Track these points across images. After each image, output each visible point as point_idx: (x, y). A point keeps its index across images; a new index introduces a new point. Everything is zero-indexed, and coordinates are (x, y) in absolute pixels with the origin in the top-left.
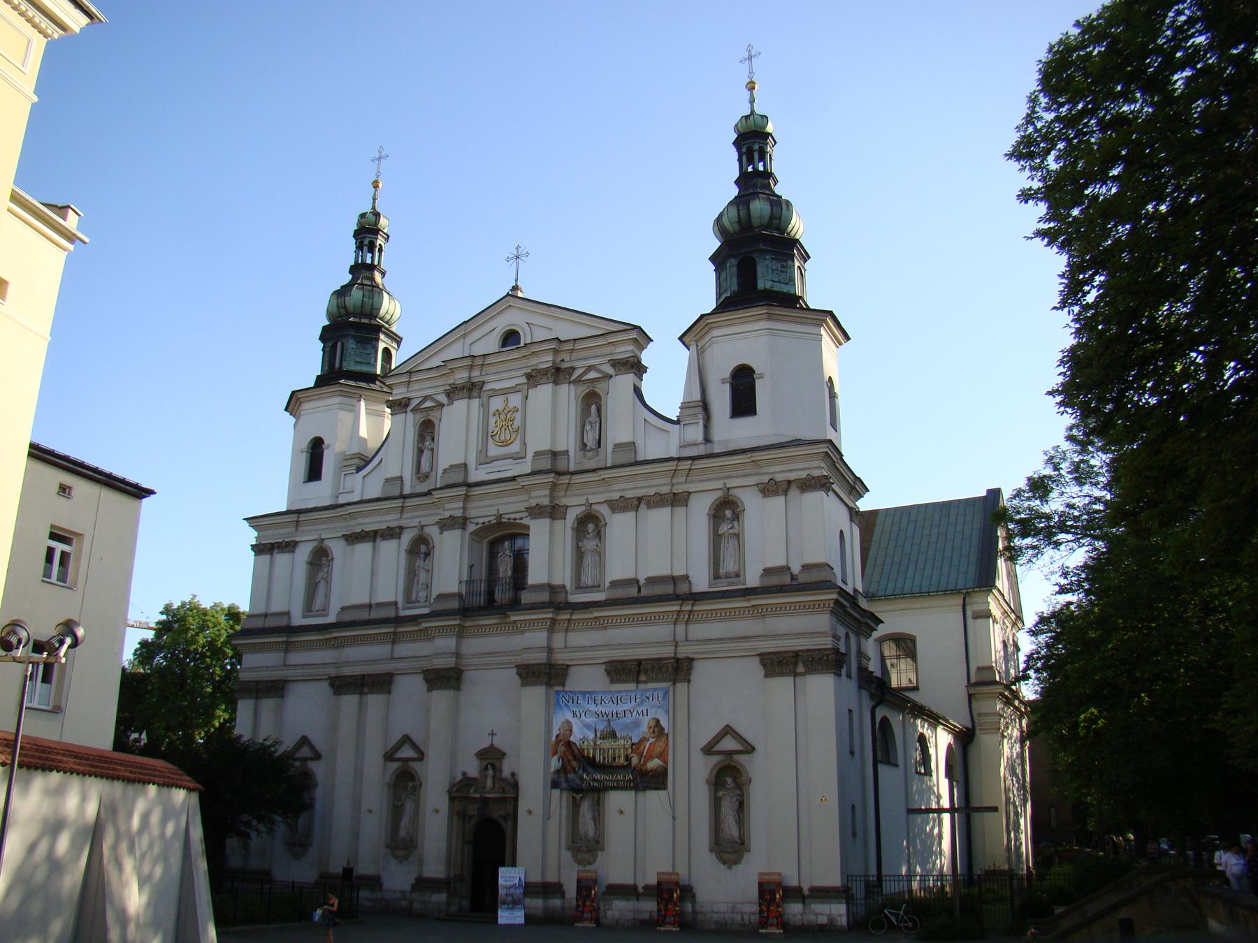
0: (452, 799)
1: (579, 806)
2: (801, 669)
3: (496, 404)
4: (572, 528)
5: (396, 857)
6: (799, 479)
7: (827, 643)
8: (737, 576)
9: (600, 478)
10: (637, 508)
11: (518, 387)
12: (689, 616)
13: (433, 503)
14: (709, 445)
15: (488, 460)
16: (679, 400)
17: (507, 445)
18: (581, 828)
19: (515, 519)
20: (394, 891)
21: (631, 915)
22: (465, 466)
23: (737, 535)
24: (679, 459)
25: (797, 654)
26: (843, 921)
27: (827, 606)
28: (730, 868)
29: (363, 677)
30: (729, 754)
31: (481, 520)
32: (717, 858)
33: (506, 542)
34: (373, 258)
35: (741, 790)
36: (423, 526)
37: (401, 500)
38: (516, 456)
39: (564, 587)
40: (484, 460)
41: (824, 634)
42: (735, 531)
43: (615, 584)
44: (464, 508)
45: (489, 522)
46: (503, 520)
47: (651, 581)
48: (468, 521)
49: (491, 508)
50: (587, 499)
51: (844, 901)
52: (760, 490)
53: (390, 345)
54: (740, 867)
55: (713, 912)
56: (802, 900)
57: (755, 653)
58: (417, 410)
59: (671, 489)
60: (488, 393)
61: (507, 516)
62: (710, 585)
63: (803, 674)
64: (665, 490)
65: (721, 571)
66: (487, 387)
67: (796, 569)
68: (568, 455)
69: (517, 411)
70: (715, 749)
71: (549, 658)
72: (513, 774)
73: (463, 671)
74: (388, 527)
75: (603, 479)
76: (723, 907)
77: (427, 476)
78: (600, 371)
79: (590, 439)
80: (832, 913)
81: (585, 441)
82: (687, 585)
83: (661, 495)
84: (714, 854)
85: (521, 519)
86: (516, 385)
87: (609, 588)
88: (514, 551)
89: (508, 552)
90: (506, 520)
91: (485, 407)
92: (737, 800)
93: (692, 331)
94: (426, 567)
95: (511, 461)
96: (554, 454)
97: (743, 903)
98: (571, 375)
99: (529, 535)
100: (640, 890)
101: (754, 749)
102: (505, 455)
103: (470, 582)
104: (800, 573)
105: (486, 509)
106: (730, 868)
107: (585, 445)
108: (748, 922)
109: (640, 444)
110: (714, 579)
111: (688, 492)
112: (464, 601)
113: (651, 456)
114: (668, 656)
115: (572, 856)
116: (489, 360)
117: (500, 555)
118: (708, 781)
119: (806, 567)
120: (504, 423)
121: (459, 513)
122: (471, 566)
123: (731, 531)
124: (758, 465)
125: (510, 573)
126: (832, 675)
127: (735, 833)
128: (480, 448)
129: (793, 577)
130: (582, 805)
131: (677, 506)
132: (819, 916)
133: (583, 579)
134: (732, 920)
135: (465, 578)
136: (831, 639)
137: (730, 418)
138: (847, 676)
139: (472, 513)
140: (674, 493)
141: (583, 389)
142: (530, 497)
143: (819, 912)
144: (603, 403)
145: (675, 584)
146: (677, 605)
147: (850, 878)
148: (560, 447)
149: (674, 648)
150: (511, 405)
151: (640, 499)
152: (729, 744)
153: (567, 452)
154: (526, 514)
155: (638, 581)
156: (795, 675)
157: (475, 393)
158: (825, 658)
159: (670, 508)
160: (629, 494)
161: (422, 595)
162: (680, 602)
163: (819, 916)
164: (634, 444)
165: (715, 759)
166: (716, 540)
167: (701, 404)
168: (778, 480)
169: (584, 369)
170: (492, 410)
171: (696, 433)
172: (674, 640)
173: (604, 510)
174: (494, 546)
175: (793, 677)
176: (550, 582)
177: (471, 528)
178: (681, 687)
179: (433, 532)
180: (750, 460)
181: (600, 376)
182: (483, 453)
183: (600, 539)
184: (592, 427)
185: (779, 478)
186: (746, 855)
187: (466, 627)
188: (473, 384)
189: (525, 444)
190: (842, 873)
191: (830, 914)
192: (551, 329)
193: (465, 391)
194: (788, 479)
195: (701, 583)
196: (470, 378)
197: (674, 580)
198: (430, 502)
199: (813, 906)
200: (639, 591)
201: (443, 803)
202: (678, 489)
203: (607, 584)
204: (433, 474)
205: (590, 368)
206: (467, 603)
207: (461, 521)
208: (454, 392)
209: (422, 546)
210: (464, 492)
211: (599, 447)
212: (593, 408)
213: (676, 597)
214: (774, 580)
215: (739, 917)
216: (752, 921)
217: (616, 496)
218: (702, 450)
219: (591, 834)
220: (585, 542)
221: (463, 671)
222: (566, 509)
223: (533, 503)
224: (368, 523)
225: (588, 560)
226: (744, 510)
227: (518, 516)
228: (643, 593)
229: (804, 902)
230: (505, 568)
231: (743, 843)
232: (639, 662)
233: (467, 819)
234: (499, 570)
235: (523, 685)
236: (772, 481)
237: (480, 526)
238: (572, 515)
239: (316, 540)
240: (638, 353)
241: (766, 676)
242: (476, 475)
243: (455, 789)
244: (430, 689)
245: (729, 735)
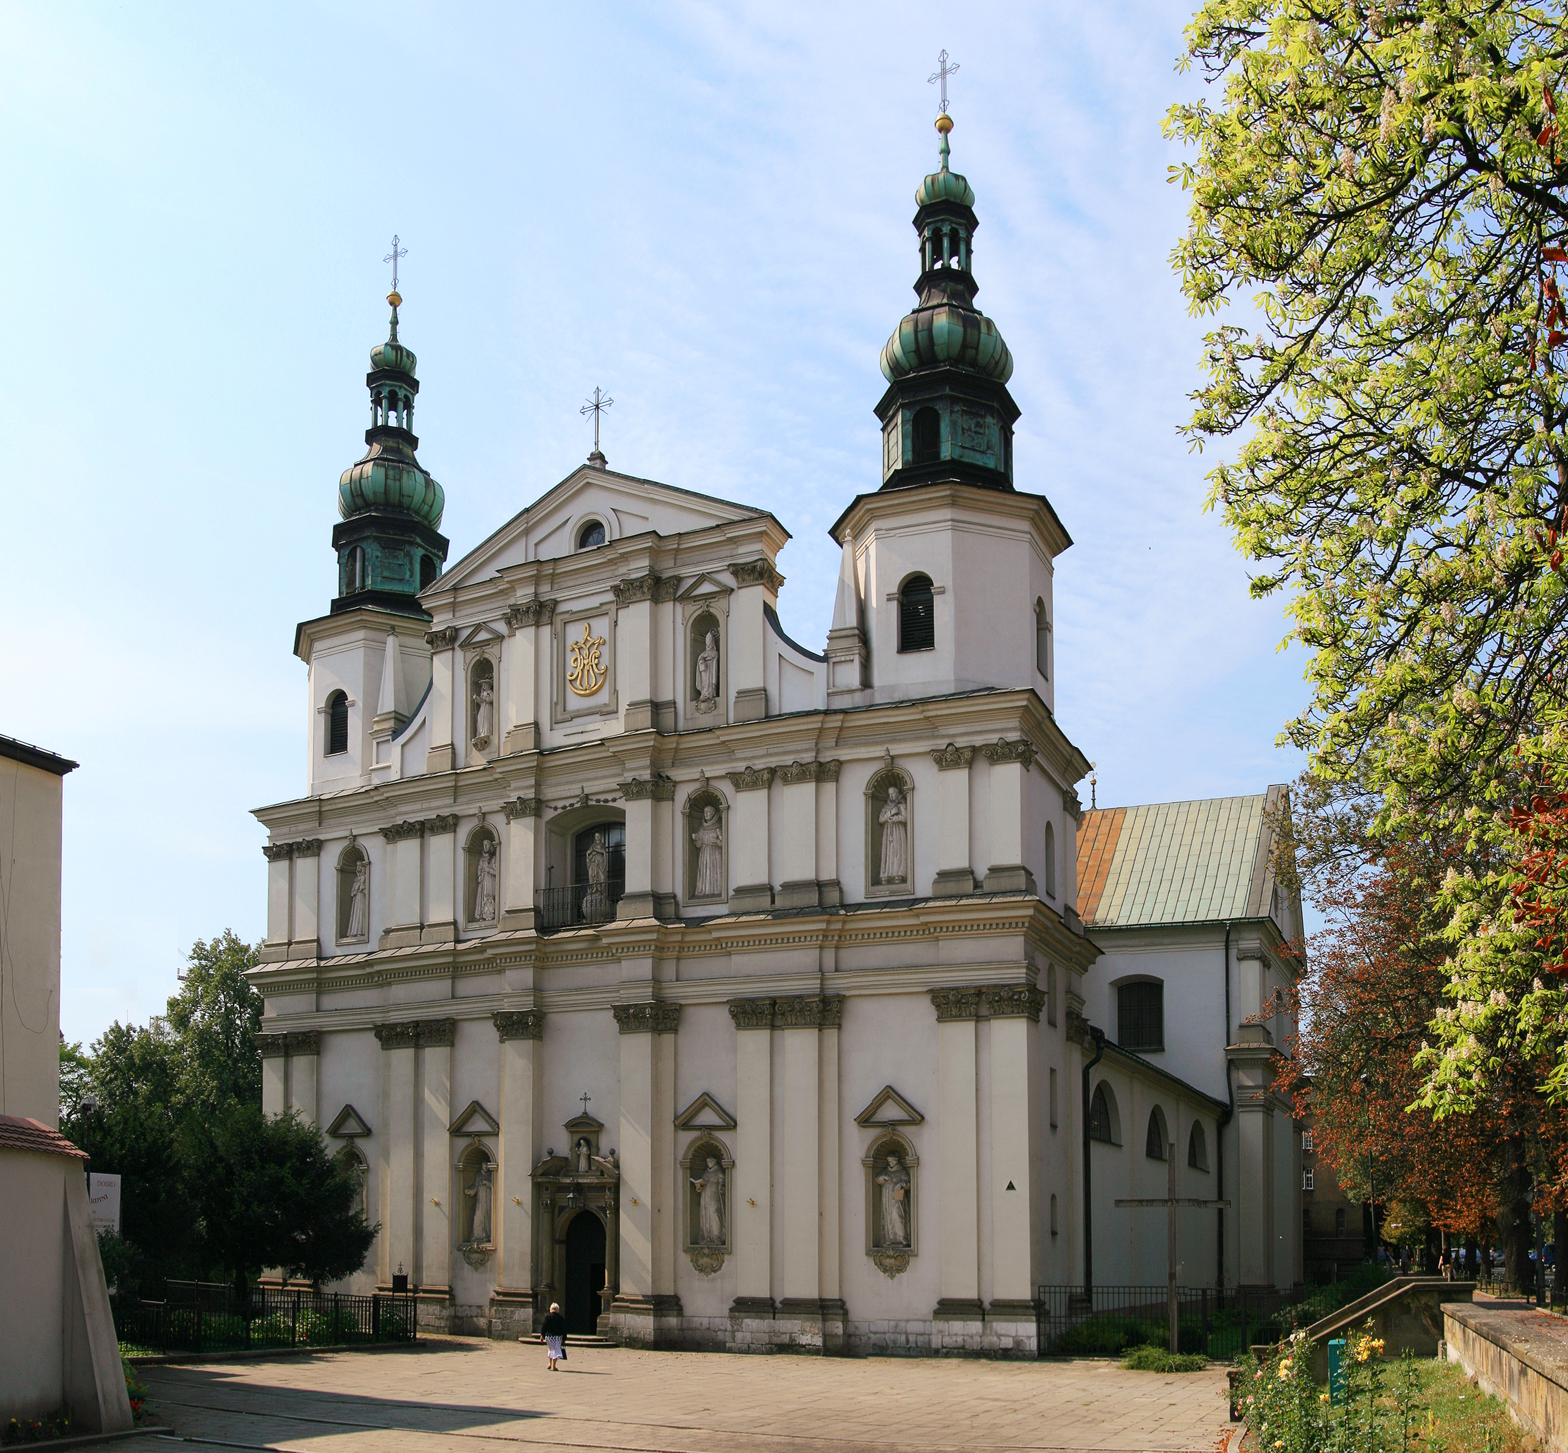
0: (538, 1187)
1: (700, 1194)
2: (984, 1011)
3: (576, 633)
4: (683, 813)
5: (470, 1264)
6: (987, 745)
7: (1018, 975)
8: (904, 880)
9: (717, 741)
10: (769, 785)
11: (604, 608)
12: (840, 937)
13: (496, 780)
14: (868, 691)
15: (568, 716)
16: (826, 623)
17: (589, 695)
18: (704, 1225)
19: (606, 801)
20: (470, 1306)
21: (766, 1338)
22: (536, 724)
23: (904, 824)
24: (826, 712)
25: (979, 992)
26: (1032, 1344)
27: (1020, 925)
28: (892, 1277)
29: (417, 1024)
30: (893, 1124)
31: (560, 804)
32: (876, 1264)
33: (597, 835)
34: (399, 418)
35: (908, 1174)
36: (484, 814)
37: (453, 777)
38: (605, 710)
39: (675, 897)
40: (562, 716)
41: (1014, 964)
42: (900, 818)
43: (741, 891)
44: (538, 785)
45: (572, 805)
46: (590, 803)
47: (789, 887)
48: (544, 805)
49: (573, 786)
50: (702, 771)
51: (1034, 1318)
52: (935, 760)
53: (431, 552)
54: (904, 1275)
55: (871, 1332)
56: (981, 1317)
57: (926, 989)
58: (469, 644)
59: (816, 757)
60: (567, 616)
61: (595, 798)
62: (867, 892)
63: (987, 1018)
64: (808, 757)
65: (882, 875)
66: (563, 608)
67: (981, 871)
68: (675, 708)
69: (604, 643)
70: (874, 1119)
71: (654, 996)
72: (613, 1152)
73: (545, 1014)
74: (438, 816)
75: (724, 742)
76: (882, 1326)
77: (486, 742)
78: (717, 583)
79: (706, 682)
80: (1019, 1333)
81: (699, 688)
82: (837, 894)
83: (801, 765)
84: (871, 1259)
85: (614, 800)
86: (601, 604)
87: (733, 898)
88: (609, 847)
89: (598, 848)
90: (594, 803)
91: (559, 638)
92: (902, 1188)
93: (847, 521)
94: (492, 871)
95: (597, 717)
96: (656, 707)
97: (907, 1321)
98: (676, 591)
99: (624, 824)
100: (778, 1304)
101: (923, 1118)
102: (589, 709)
103: (549, 890)
104: (985, 878)
105: (567, 787)
106: (892, 1277)
107: (698, 693)
108: (914, 1345)
109: (773, 691)
110: (873, 885)
111: (838, 760)
112: (543, 916)
113: (787, 709)
114: (809, 992)
115: (692, 1261)
116: (563, 568)
117: (589, 852)
118: (864, 1163)
119: (994, 870)
120: (586, 662)
121: (530, 794)
122: (550, 869)
123: (895, 819)
124: (933, 724)
125: (602, 877)
126: (1025, 1020)
127: (900, 1233)
128: (555, 700)
129: (977, 885)
130: (703, 1194)
131: (825, 780)
132: (1002, 1338)
133: (699, 884)
134: (894, 1342)
135: (543, 887)
136: (1024, 971)
137: (898, 652)
138: (1049, 1022)
139: (549, 793)
140: (821, 764)
141: (694, 610)
142: (624, 770)
143: (1003, 1332)
144: (722, 630)
145: (820, 893)
146: (822, 921)
147: (1042, 1290)
148: (666, 696)
149: (819, 981)
150: (595, 635)
151: (773, 771)
152: (891, 1112)
153: (675, 703)
154: (620, 794)
155: (771, 888)
156: (978, 1018)
157: (545, 619)
158: (1016, 997)
159: (813, 784)
160: (759, 765)
161: (488, 909)
162: (826, 917)
163: (1002, 1338)
164: (765, 690)
165: (872, 1133)
166: (876, 831)
167: (857, 632)
168: (957, 745)
169: (691, 581)
170: (570, 642)
171: (850, 675)
172: (820, 970)
173: (726, 788)
174: (582, 840)
175: (973, 1023)
176: (655, 889)
177: (549, 814)
178: (831, 1034)
179: (498, 821)
180: (921, 716)
181: (715, 589)
182: (560, 708)
183: (721, 829)
184: (706, 666)
185: (961, 742)
186: (912, 1260)
187: (546, 953)
188: (542, 605)
189: (616, 691)
190: (1033, 1284)
191: (1017, 1335)
192: (647, 519)
193: (531, 615)
194: (973, 744)
195: (856, 888)
196: (536, 594)
197: (819, 885)
198: (490, 778)
199: (994, 1324)
200: (773, 902)
201: (525, 1192)
202: (826, 757)
203: (731, 893)
204: (495, 739)
205: (702, 578)
206: (546, 920)
207: (533, 805)
208: (515, 616)
209: (485, 842)
210: (535, 763)
211: (718, 695)
212: (709, 637)
213: (823, 909)
214: (952, 887)
215: (903, 1338)
216: (919, 1344)
217: (740, 766)
218: (858, 699)
219: (715, 1231)
220: (701, 833)
221: (545, 1014)
222: (674, 786)
223: (628, 777)
224: (413, 812)
225: (706, 857)
226: (913, 788)
227: (609, 797)
228: (779, 903)
229: (984, 1320)
230: (596, 869)
231: (909, 1246)
232: (774, 1001)
233: (557, 1210)
234: (587, 874)
235: (622, 1031)
236: (950, 748)
237: (559, 811)
238: (682, 794)
239: (346, 837)
240: (771, 556)
241: (940, 1020)
242: (554, 738)
243: (540, 1172)
244: (502, 1041)
245: (890, 1101)
